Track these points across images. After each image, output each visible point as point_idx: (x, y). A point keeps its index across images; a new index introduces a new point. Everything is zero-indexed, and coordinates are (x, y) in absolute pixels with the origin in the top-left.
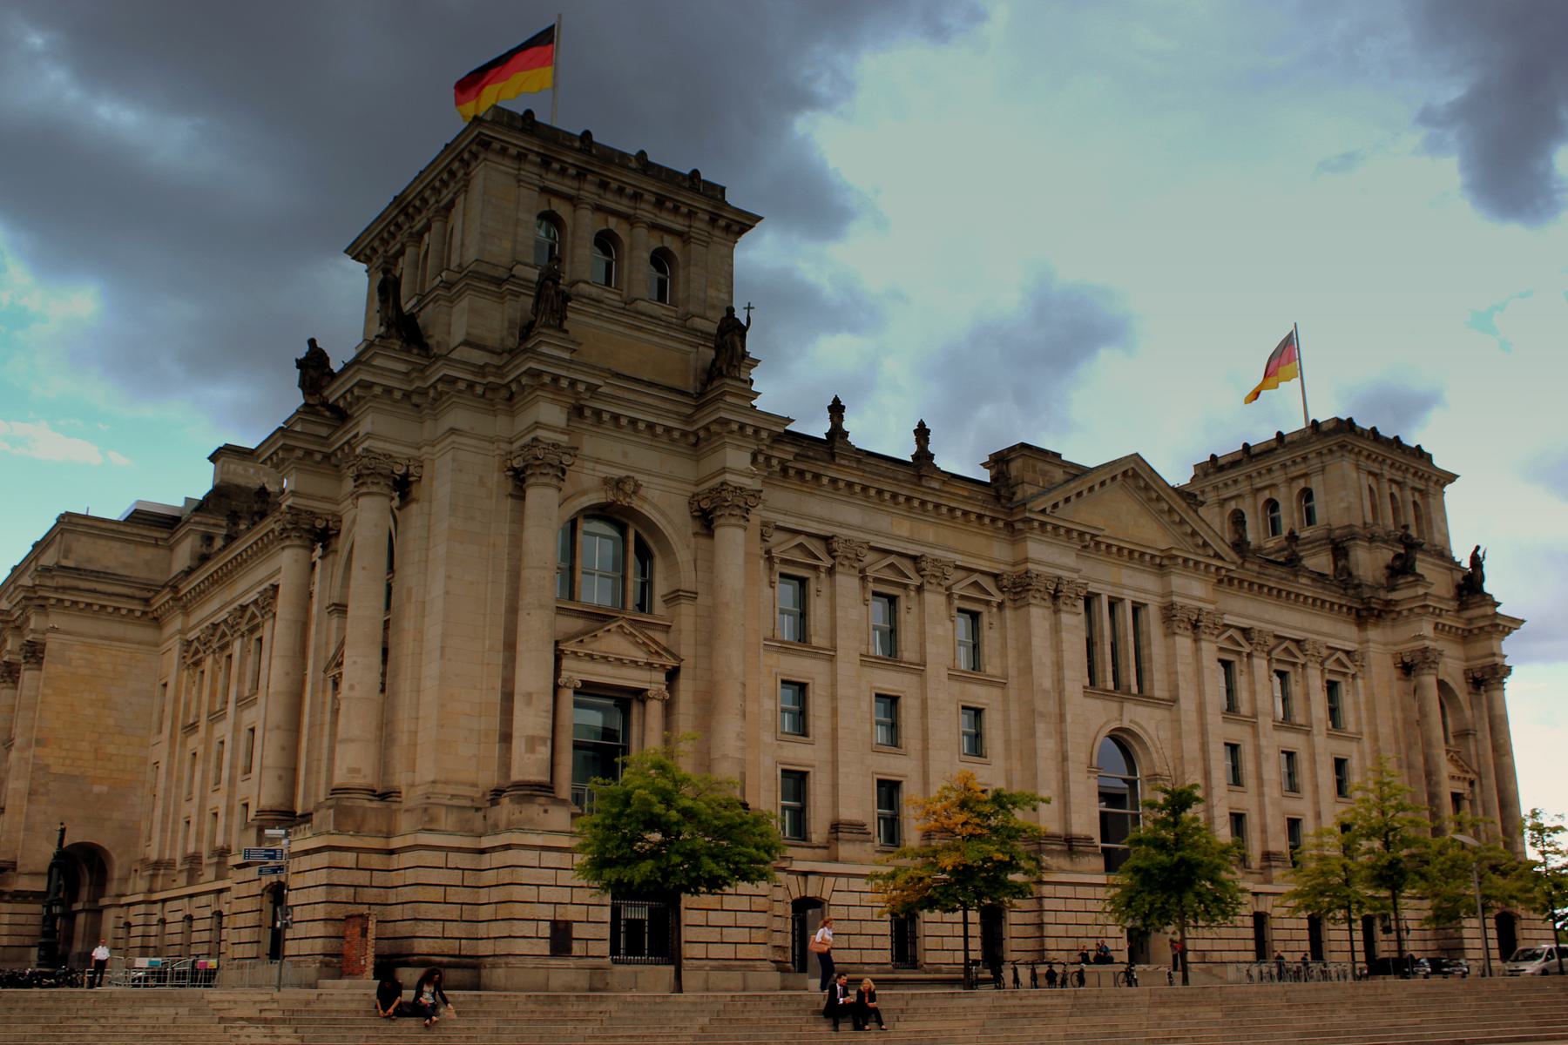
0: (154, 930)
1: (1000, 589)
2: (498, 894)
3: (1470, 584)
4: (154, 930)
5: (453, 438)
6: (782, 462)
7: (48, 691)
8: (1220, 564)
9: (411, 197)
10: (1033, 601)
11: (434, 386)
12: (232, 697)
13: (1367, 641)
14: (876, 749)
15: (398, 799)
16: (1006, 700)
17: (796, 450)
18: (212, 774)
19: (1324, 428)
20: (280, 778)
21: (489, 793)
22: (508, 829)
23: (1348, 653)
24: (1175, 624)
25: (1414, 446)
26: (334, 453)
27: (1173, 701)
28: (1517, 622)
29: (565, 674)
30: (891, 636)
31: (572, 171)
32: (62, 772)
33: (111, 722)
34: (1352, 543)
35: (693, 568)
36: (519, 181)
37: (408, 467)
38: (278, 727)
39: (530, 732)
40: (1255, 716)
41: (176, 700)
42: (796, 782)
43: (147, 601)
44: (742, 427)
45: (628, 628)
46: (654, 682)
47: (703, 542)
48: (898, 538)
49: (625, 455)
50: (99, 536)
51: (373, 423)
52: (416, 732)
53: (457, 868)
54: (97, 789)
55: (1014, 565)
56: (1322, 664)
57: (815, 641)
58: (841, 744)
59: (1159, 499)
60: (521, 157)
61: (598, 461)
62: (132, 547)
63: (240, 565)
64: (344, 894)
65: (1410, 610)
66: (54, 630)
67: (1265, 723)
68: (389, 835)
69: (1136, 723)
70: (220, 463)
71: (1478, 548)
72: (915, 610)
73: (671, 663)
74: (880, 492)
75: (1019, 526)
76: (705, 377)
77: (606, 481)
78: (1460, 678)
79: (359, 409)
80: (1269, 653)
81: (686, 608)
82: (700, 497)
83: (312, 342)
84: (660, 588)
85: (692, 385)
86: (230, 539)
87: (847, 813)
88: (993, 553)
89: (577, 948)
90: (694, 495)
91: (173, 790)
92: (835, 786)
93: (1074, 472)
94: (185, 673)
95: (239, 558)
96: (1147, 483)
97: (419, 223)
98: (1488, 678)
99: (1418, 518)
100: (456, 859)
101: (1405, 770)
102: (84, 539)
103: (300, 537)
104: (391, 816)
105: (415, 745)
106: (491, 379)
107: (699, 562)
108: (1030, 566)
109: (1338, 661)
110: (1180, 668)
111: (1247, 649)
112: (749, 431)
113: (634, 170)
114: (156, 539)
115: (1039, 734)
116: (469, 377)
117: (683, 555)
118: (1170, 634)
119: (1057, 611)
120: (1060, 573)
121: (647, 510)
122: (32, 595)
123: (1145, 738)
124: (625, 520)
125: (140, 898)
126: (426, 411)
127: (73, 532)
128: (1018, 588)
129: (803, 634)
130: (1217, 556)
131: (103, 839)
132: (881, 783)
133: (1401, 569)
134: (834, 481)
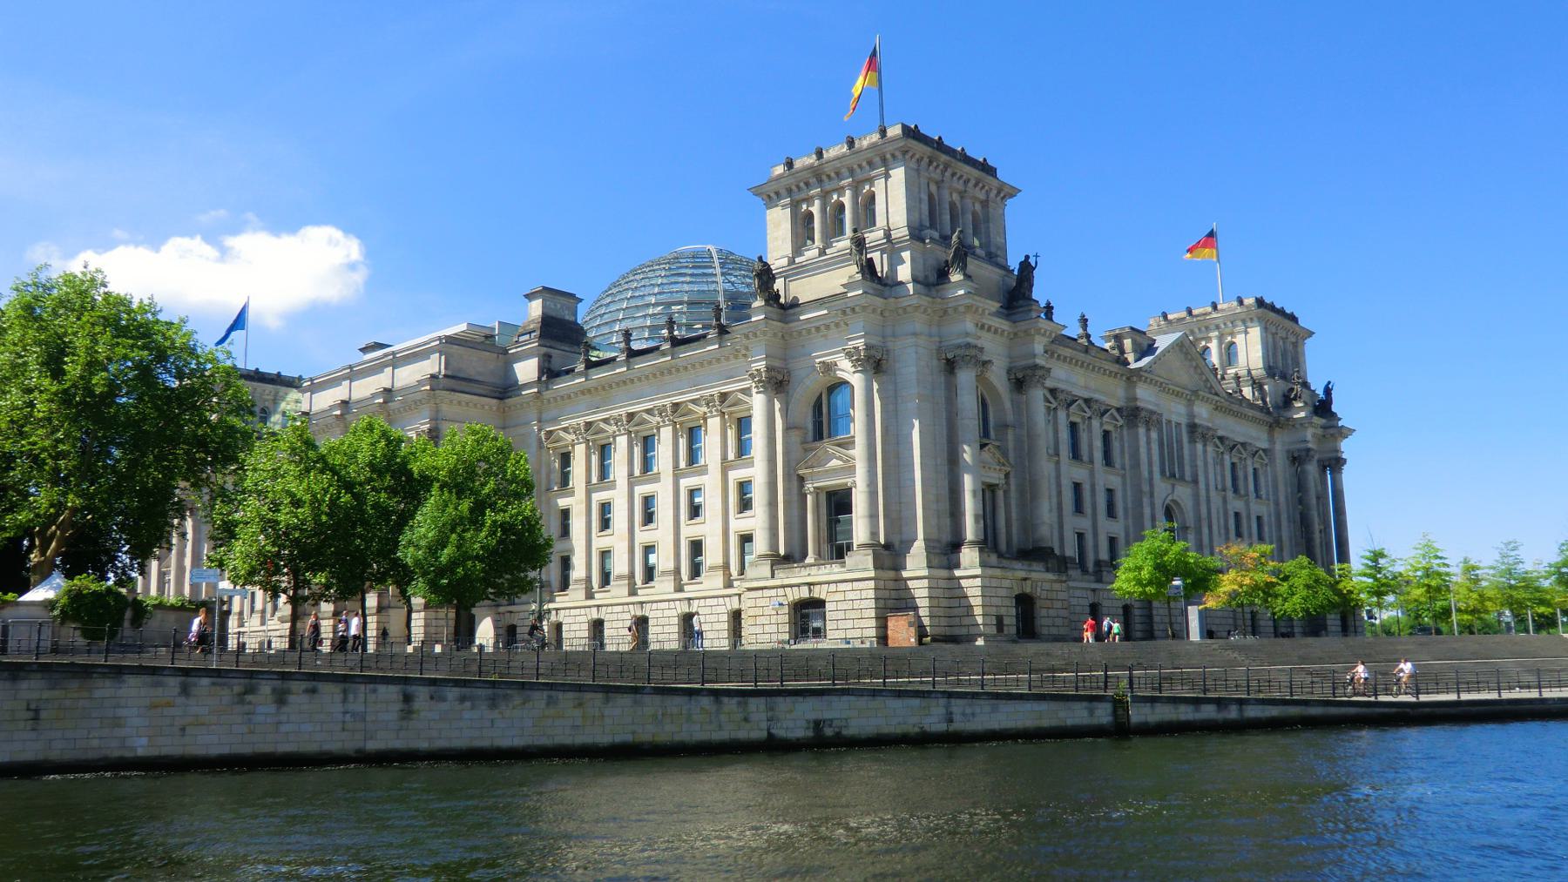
3: (1323, 407)
8: (1216, 398)
11: (904, 309)
16: (1124, 484)
23: (1264, 450)
27: (1195, 481)
36: (919, 174)
45: (992, 450)
71: (1329, 383)
75: (1135, 379)
98: (1335, 463)
108: (1139, 404)
113: (960, 160)
116: (926, 304)
118: (1192, 441)
123: (1182, 504)
130: (1216, 394)
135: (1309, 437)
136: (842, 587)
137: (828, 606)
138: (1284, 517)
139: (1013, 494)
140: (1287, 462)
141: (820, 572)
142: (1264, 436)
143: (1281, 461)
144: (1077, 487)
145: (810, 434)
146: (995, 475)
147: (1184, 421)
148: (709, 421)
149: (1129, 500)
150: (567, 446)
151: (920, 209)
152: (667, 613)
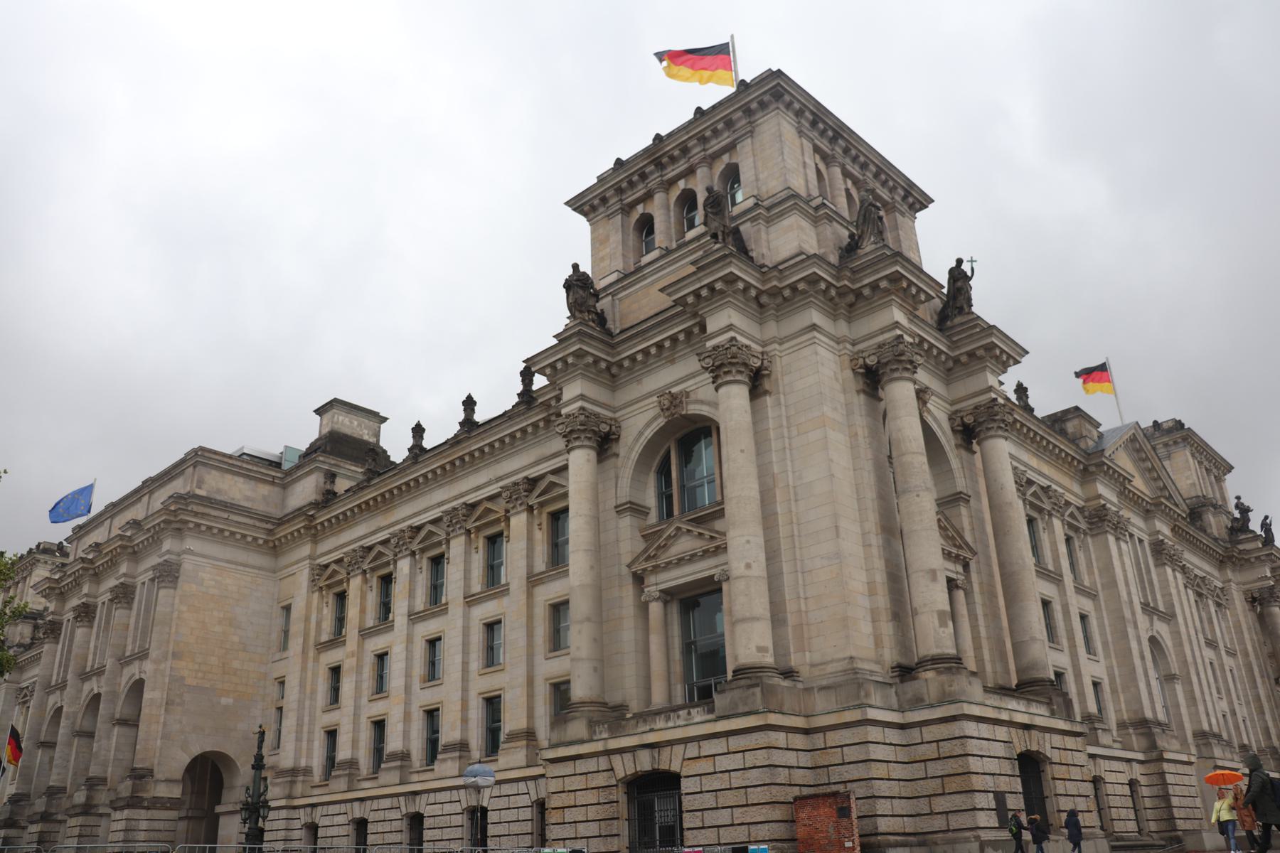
0: (296, 834)
2: (936, 769)
5: (816, 334)
7: (184, 608)
9: (668, 148)
10: (1108, 529)
11: (793, 287)
13: (1230, 581)
15: (800, 679)
16: (1098, 609)
19: (1165, 426)
20: (595, 669)
21: (890, 670)
24: (1164, 556)
26: (619, 364)
27: (1169, 617)
31: (830, 133)
32: (195, 684)
33: (236, 639)
34: (1204, 509)
35: (962, 475)
37: (762, 360)
38: (588, 619)
43: (270, 532)
47: (963, 453)
50: (227, 471)
51: (730, 317)
52: (806, 612)
53: (891, 744)
54: (224, 701)
55: (1086, 501)
59: (1147, 459)
60: (799, 114)
62: (253, 482)
64: (782, 776)
65: (1258, 558)
66: (190, 552)
69: (1158, 632)
70: (327, 416)
71: (1266, 518)
76: (936, 317)
79: (709, 305)
81: (964, 510)
82: (965, 414)
83: (575, 267)
88: (1070, 489)
90: (956, 412)
91: (307, 703)
94: (316, 595)
95: (141, 546)
97: (671, 173)
102: (214, 472)
103: (589, 439)
106: (846, 282)
107: (966, 470)
109: (1218, 596)
114: (274, 477)
117: (955, 463)
118: (1160, 564)
122: (172, 519)
125: (283, 803)
126: (770, 313)
127: (205, 465)
128: (1098, 519)
130: (1176, 505)
136: (710, 747)
137: (687, 785)
139: (978, 598)
140: (1247, 607)
141: (671, 724)
144: (1046, 604)
145: (653, 518)
147: (1146, 538)
148: (513, 521)
149: (1108, 630)
150: (341, 582)
151: (806, 175)
152: (448, 808)
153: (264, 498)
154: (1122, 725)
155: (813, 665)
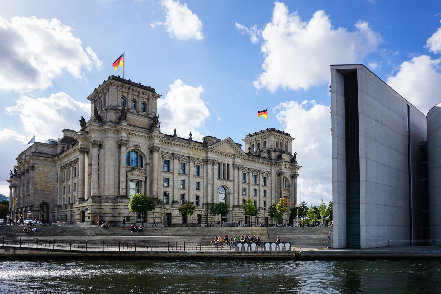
1: (203, 162)
4: (59, 217)
6: (164, 141)
8: (244, 157)
12: (71, 177)
14: (181, 189)
16: (203, 181)
17: (167, 139)
18: (68, 190)
22: (120, 203)
23: (269, 172)
25: (287, 133)
27: (234, 180)
28: (301, 167)
29: (128, 178)
30: (184, 170)
38: (81, 185)
39: (122, 188)
40: (249, 183)
41: (60, 177)
42: (167, 195)
43: (53, 158)
44: (157, 136)
45: (138, 170)
46: (143, 179)
47: (151, 155)
48: (185, 153)
49: (137, 141)
56: (263, 174)
57: (170, 171)
58: (174, 188)
61: (133, 142)
63: (71, 154)
65: (280, 165)
67: (251, 184)
68: (101, 203)
72: (188, 166)
73: (145, 176)
74: (182, 146)
75: (207, 151)
77: (134, 145)
78: (289, 176)
80: (253, 172)
84: (144, 163)
85: (149, 128)
86: (68, 148)
87: (175, 200)
88: (202, 155)
89: (130, 220)
92: (173, 195)
93: (218, 140)
96: (231, 143)
98: (294, 176)
99: (285, 147)
100: (111, 207)
101: (276, 193)
104: (101, 200)
105: (104, 189)
108: (209, 158)
110: (235, 175)
111: (249, 171)
112: (158, 137)
115: (209, 187)
117: (148, 158)
118: (234, 169)
119: (213, 166)
120: (214, 159)
121: (141, 150)
123: (228, 187)
124: (138, 151)
128: (206, 161)
129: (168, 171)
130: (244, 156)
131: (48, 201)
132: (181, 195)
133: (280, 157)
134: (174, 144)
135: (283, 167)
138: (274, 191)
142: (270, 168)
143: (274, 175)
146: (142, 178)
147: (231, 164)
149: (205, 185)
153: (52, 151)
154: (203, 204)
155: (104, 195)
